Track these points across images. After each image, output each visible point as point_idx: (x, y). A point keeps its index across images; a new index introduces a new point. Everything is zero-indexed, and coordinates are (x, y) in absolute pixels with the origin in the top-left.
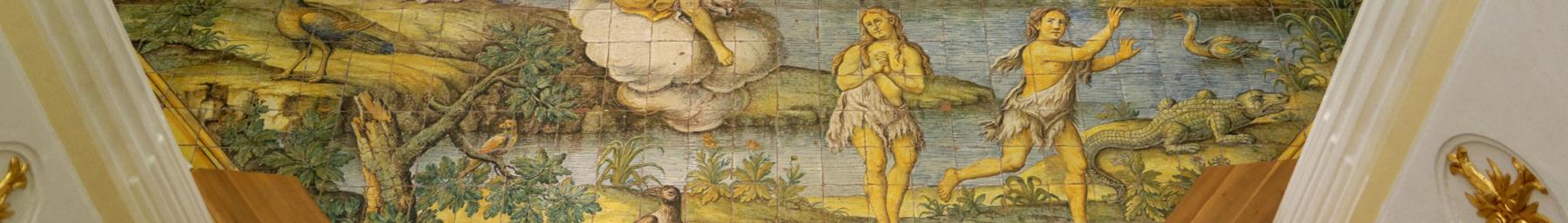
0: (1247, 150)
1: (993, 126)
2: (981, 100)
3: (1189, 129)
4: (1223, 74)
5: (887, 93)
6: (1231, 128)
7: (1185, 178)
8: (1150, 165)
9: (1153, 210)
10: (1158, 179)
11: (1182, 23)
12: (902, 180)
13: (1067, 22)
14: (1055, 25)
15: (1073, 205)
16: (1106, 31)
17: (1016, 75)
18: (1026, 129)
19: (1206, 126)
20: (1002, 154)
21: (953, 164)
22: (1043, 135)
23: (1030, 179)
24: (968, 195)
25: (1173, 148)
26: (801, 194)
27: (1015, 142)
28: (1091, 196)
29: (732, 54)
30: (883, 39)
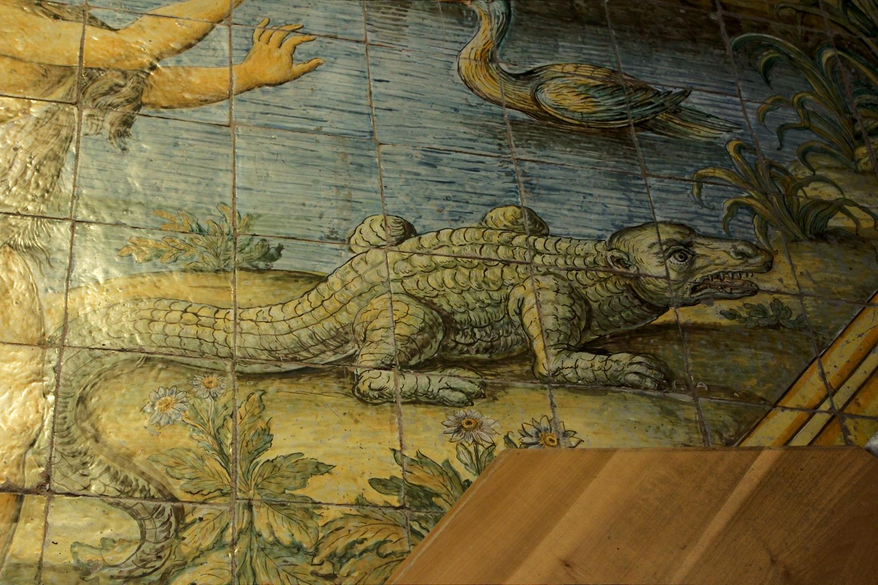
0: (641, 411)
3: (448, 323)
4: (570, 166)
6: (587, 332)
7: (418, 499)
10: (317, 488)
19: (504, 315)
25: (385, 380)
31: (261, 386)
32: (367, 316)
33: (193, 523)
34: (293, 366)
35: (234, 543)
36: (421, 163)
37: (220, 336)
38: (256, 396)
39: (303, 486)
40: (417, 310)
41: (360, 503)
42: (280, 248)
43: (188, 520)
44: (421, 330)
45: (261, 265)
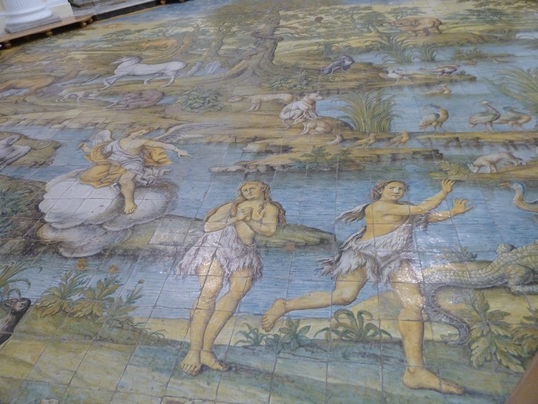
1: (330, 263)
2: (323, 242)
5: (241, 235)
8: (496, 304)
9: (505, 355)
10: (507, 320)
11: (509, 189)
12: (229, 308)
13: (406, 188)
14: (396, 190)
15: (407, 344)
16: (441, 194)
17: (358, 225)
18: (361, 267)
20: (335, 288)
21: (284, 295)
22: (378, 272)
23: (360, 313)
24: (292, 325)
25: (519, 288)
26: (130, 314)
27: (349, 277)
28: (428, 335)
29: (136, 207)
30: (252, 199)
31: (482, 291)
32: (508, 271)
33: (473, 329)
34: (490, 286)
35: (487, 335)
36: (511, 229)
37: (466, 279)
38: (481, 295)
39: (503, 319)
40: (523, 269)
41: (522, 323)
42: (476, 255)
43: (472, 328)
44: (526, 274)
45: (472, 259)
